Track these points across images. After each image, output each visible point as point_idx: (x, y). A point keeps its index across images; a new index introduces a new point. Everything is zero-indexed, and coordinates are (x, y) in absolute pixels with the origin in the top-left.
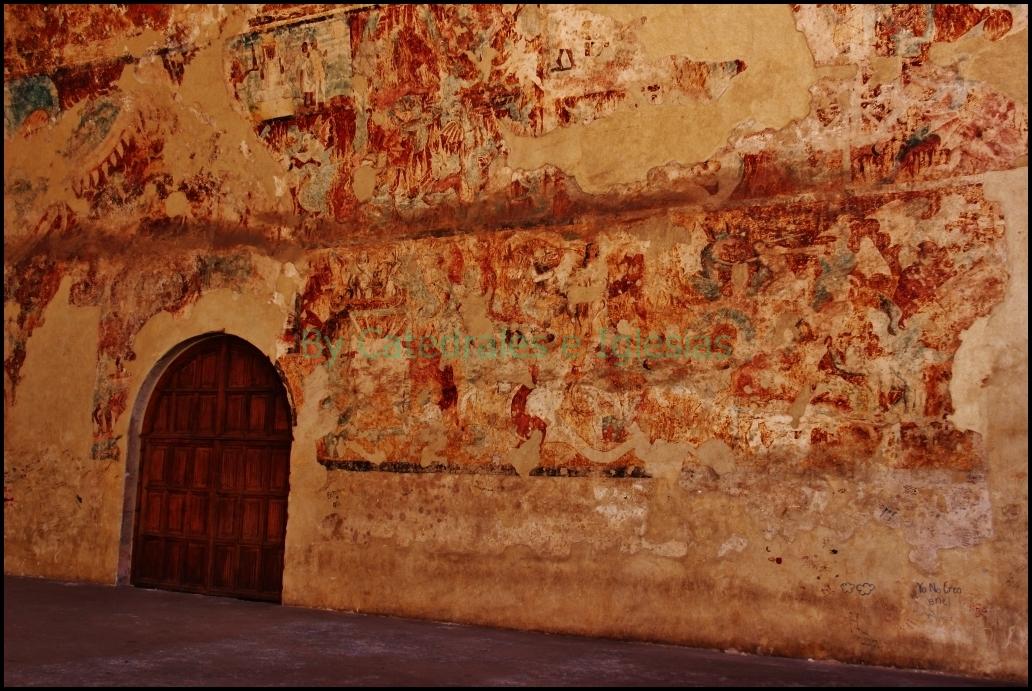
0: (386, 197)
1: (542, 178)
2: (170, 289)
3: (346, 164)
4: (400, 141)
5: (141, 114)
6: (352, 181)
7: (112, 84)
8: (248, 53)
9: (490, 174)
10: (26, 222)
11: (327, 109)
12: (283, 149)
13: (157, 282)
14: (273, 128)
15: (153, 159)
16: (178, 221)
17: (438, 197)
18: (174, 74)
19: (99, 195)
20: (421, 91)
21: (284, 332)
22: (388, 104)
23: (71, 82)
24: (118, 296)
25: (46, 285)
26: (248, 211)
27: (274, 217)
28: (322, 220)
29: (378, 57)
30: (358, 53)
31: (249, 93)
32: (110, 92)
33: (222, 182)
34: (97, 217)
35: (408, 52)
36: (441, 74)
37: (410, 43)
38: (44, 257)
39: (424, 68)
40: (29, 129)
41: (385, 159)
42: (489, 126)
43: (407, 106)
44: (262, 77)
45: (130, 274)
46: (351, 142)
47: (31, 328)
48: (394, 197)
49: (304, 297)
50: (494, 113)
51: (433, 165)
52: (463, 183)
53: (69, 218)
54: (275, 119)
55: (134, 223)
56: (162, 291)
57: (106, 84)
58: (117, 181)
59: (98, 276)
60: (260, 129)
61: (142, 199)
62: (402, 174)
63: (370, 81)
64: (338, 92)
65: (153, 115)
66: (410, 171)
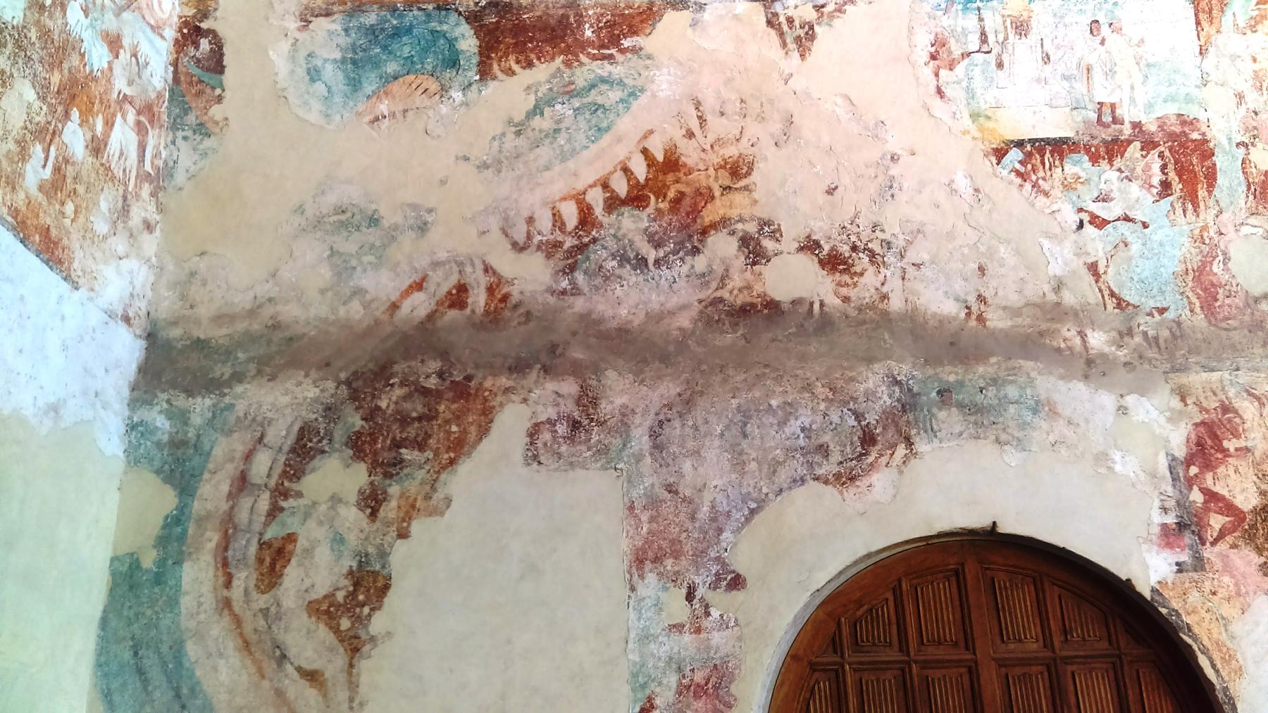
2: (826, 438)
3: (1204, 228)
5: (698, 105)
6: (1227, 259)
7: (626, 43)
8: (971, 22)
10: (359, 292)
12: (1057, 192)
13: (783, 423)
14: (1029, 155)
15: (726, 189)
16: (806, 307)
18: (789, 40)
19: (582, 248)
21: (1156, 530)
23: (520, 29)
24: (674, 449)
25: (447, 422)
26: (981, 299)
27: (1056, 312)
32: (619, 57)
33: (909, 243)
34: (575, 291)
38: (434, 365)
40: (384, 107)
44: (1000, 65)
45: (702, 403)
46: (1210, 192)
47: (408, 518)
49: (1188, 462)
53: (491, 290)
54: (1033, 141)
55: (684, 307)
56: (802, 442)
57: (615, 41)
58: (632, 224)
59: (606, 408)
60: (1000, 154)
61: (700, 263)
64: (1171, 110)
65: (729, 109)
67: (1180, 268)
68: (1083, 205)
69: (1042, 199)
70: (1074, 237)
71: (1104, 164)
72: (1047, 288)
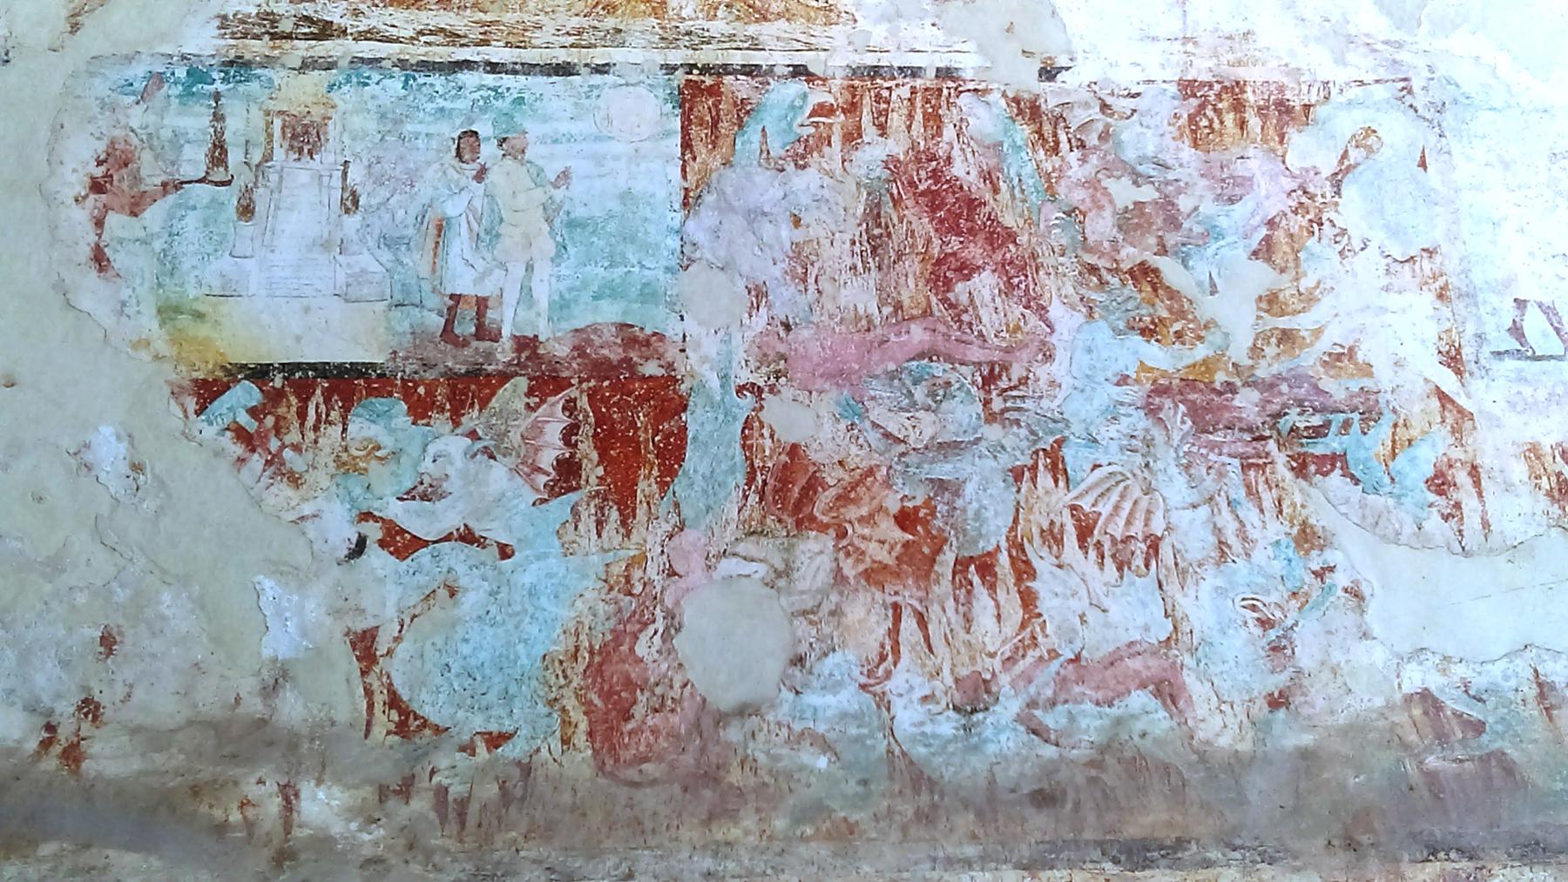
0: (848, 698)
1: (1531, 692)
3: (640, 560)
4: (893, 506)
9: (1306, 654)
11: (555, 363)
17: (1091, 723)
20: (975, 353)
22: (839, 376)
28: (526, 769)
29: (797, 222)
30: (709, 199)
31: (168, 264)
35: (924, 225)
36: (1056, 311)
37: (933, 201)
39: (985, 284)
41: (826, 563)
42: (1268, 499)
43: (920, 393)
46: (664, 486)
48: (883, 702)
50: (1281, 459)
51: (1046, 604)
52: (1189, 679)
62: (909, 624)
63: (759, 294)
64: (609, 313)
66: (944, 617)
67: (561, 647)
68: (375, 506)
69: (284, 490)
70: (336, 572)
71: (440, 422)
72: (247, 686)
